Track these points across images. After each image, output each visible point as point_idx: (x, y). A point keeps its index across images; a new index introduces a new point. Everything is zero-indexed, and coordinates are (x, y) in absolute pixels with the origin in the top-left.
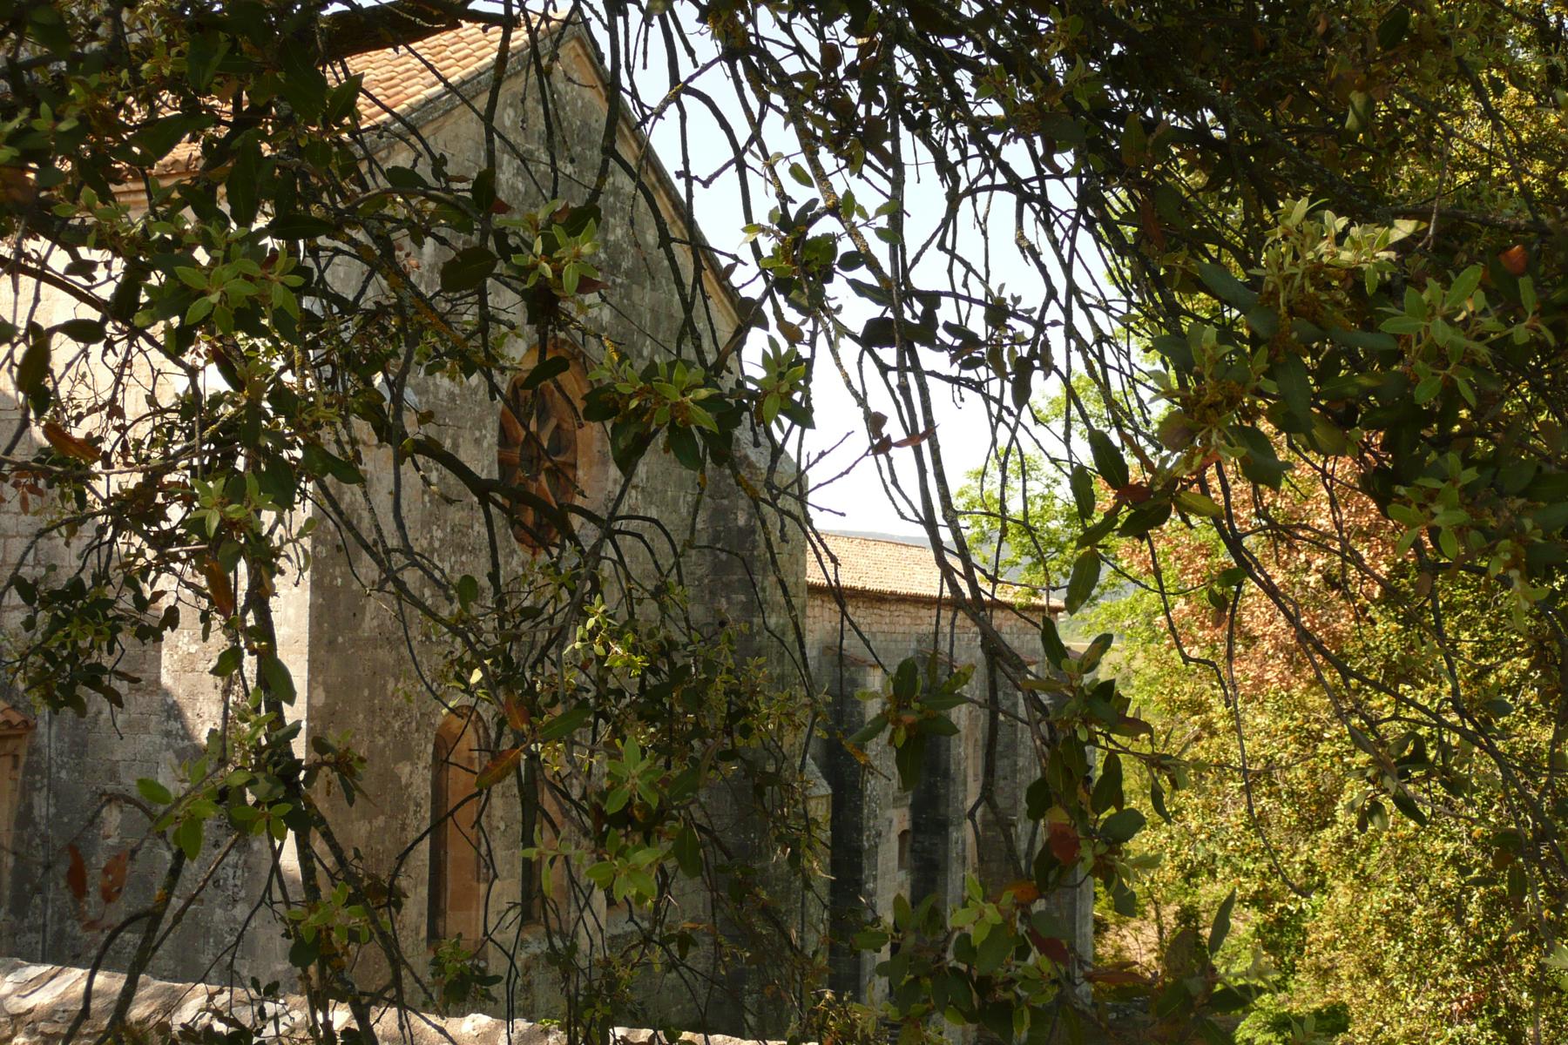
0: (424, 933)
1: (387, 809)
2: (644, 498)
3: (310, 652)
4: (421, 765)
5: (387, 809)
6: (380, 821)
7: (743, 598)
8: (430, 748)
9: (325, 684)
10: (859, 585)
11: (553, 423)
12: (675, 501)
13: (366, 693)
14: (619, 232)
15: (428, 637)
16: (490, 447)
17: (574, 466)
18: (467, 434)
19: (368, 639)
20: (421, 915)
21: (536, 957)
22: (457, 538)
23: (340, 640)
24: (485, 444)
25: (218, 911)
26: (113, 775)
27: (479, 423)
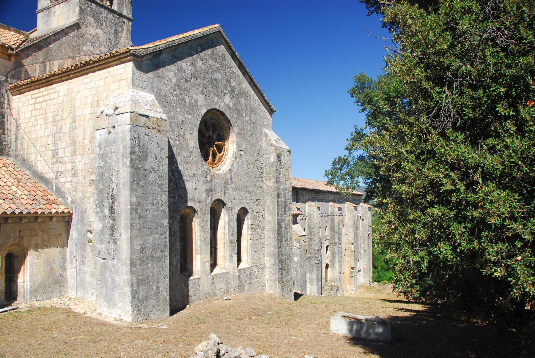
0: (179, 268)
1: (160, 232)
2: (244, 154)
3: (130, 186)
4: (176, 222)
5: (160, 232)
6: (157, 236)
7: (273, 180)
8: (179, 217)
9: (136, 195)
10: (314, 188)
11: (217, 133)
12: (254, 155)
13: (151, 199)
14: (234, 83)
15: (177, 186)
16: (195, 136)
17: (224, 145)
18: (188, 131)
19: (151, 184)
20: (178, 263)
21: (216, 275)
22: (186, 160)
23: (141, 183)
24: (194, 135)
25: (110, 262)
26: (90, 226)
27: (192, 129)
